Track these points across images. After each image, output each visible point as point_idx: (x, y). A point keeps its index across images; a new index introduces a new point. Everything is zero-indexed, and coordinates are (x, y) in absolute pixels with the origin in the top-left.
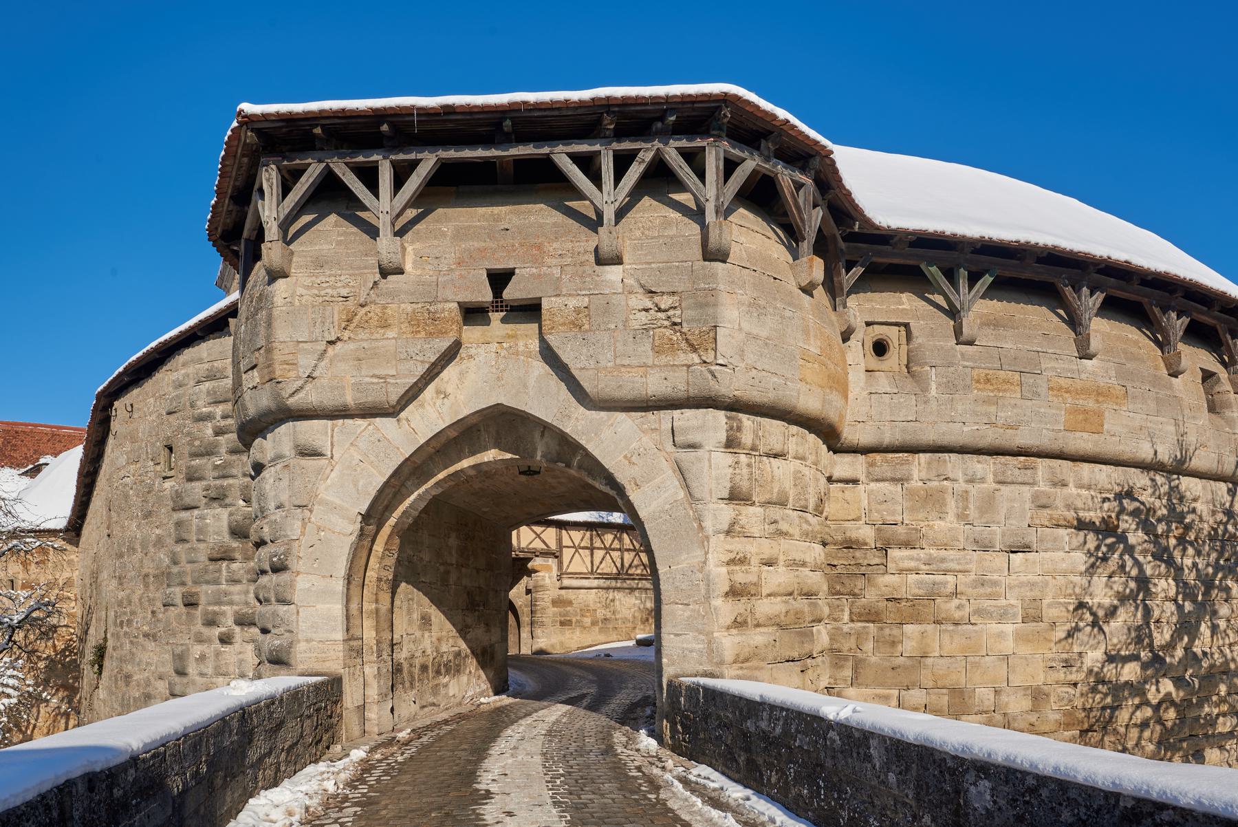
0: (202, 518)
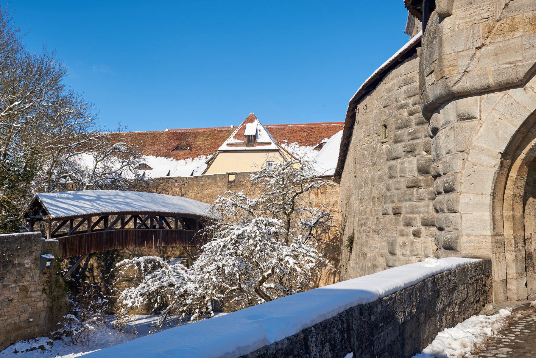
0: (402, 163)
